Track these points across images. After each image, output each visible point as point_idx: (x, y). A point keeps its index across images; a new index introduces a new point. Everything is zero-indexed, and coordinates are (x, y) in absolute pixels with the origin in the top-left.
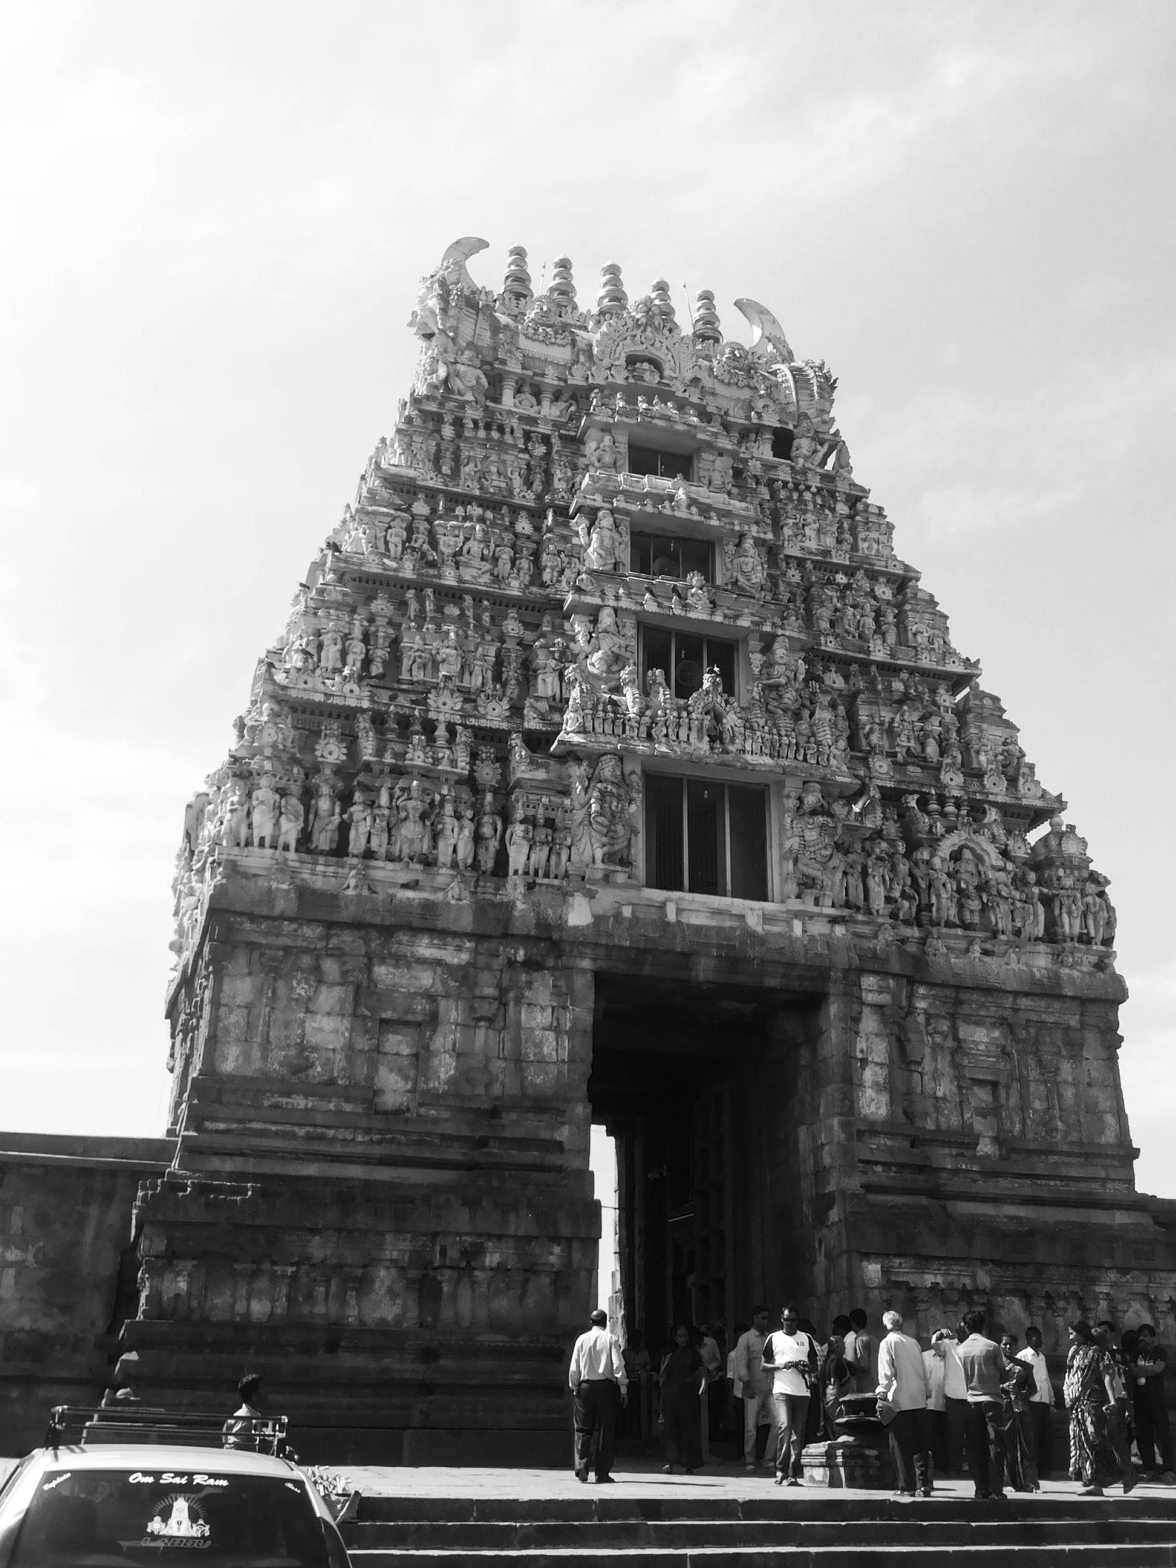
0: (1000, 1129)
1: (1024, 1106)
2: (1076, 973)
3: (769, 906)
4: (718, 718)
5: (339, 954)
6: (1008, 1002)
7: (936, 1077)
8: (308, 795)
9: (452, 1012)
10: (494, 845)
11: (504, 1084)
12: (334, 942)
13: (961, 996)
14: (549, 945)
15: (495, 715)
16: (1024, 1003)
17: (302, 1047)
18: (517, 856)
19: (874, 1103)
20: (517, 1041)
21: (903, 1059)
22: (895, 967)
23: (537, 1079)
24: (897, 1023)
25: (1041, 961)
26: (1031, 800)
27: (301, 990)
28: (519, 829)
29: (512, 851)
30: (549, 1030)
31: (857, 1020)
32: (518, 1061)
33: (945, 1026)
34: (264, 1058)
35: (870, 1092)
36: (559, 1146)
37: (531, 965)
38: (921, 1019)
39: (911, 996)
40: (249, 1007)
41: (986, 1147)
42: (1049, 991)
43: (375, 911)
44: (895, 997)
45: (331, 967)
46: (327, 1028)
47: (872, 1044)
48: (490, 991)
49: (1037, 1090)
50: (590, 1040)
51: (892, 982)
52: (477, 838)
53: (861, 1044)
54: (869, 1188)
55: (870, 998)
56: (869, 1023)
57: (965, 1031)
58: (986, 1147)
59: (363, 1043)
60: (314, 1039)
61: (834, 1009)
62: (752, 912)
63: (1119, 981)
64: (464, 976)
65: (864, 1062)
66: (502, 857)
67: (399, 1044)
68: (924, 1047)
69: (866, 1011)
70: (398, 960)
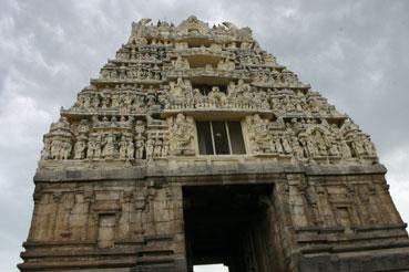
0: (352, 224)
1: (359, 215)
2: (365, 165)
3: (246, 156)
4: (219, 100)
5: (82, 193)
6: (344, 178)
7: (322, 208)
8: (73, 142)
9: (127, 208)
10: (142, 149)
11: (150, 233)
12: (81, 188)
13: (325, 178)
14: (161, 181)
15: (140, 112)
16: (349, 178)
17: (68, 227)
18: (149, 152)
19: (300, 221)
20: (153, 214)
21: (310, 204)
22: (299, 170)
23: (163, 229)
24: (304, 191)
25: (353, 163)
26: (336, 116)
27: (68, 206)
28: (149, 142)
29: (147, 149)
30: (167, 211)
31: (288, 191)
32: (154, 222)
33: (321, 189)
34: (53, 233)
35: (298, 217)
36: (172, 252)
37: (157, 187)
38: (313, 189)
39: (307, 181)
40: (48, 215)
41: (348, 231)
42: (357, 173)
43: (95, 175)
44: (301, 181)
45: (80, 198)
46: (78, 216)
47: (295, 198)
48: (142, 198)
49: (363, 208)
50: (181, 210)
51: (299, 176)
52: (136, 148)
53: (292, 199)
54: (304, 252)
55: (291, 183)
56: (293, 191)
57: (331, 190)
58: (348, 231)
59: (91, 223)
60: (73, 223)
61: (278, 187)
62: (241, 158)
63: (383, 166)
64: (130, 197)
65: (293, 206)
66: (144, 152)
67: (107, 222)
68: (314, 197)
69: (291, 188)
70: (106, 192)
